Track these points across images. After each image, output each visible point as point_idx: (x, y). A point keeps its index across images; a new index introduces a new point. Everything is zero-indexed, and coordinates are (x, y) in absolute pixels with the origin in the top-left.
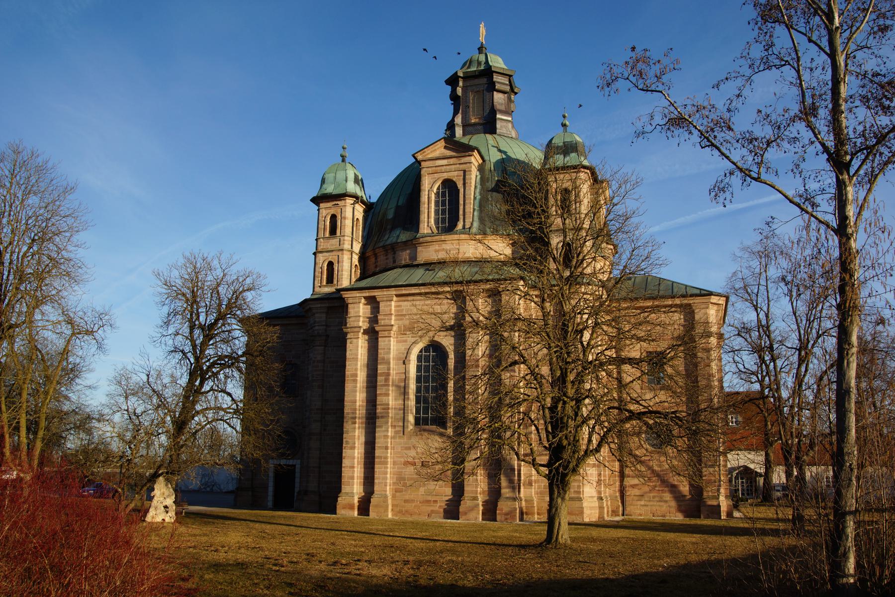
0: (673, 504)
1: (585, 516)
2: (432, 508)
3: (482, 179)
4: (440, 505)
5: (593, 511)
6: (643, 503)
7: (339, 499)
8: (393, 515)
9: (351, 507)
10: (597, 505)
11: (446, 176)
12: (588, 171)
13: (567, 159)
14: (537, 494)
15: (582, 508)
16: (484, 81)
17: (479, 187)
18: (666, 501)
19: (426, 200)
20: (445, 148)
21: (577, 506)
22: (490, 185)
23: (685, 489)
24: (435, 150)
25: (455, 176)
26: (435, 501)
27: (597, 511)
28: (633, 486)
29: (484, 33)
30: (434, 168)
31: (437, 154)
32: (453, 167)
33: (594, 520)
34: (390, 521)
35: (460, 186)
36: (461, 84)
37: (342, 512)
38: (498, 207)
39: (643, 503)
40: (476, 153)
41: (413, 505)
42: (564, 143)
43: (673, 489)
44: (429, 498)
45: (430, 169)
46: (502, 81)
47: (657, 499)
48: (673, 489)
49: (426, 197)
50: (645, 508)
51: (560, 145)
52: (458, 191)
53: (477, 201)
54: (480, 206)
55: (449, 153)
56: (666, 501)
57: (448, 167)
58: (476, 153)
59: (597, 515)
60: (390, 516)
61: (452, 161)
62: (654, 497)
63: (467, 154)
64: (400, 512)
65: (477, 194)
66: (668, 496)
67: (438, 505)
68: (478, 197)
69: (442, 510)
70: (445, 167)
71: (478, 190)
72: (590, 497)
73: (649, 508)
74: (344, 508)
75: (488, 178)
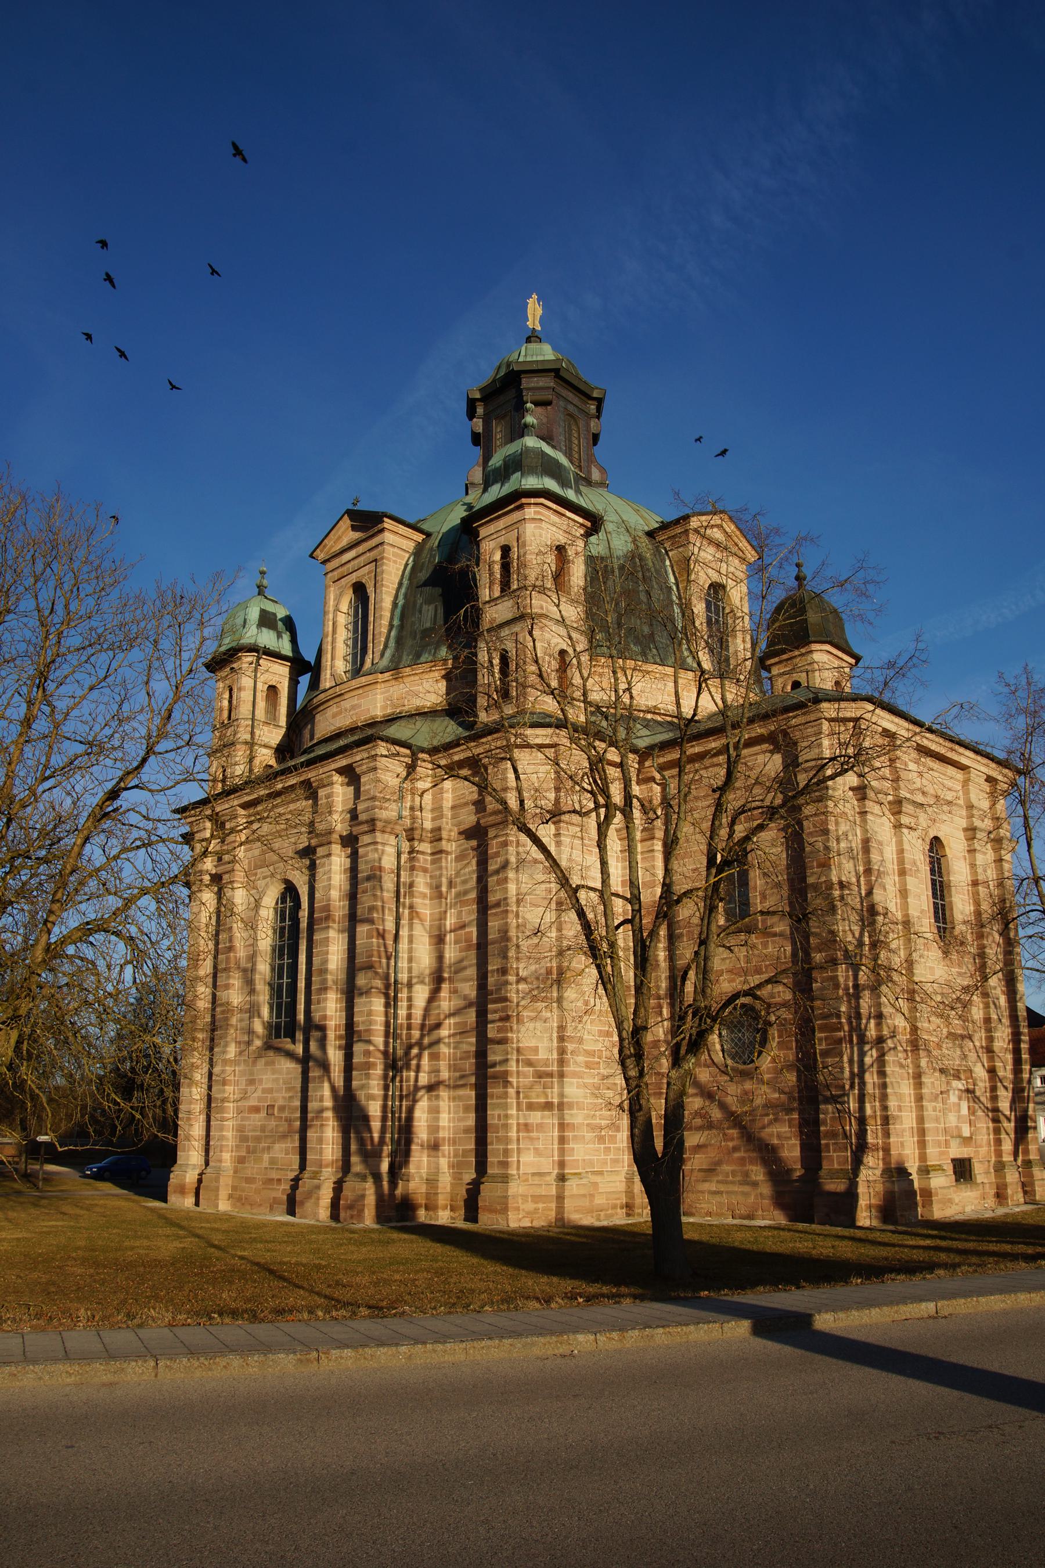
0: (766, 1189)
1: (511, 1215)
2: (274, 1194)
3: (413, 568)
4: (281, 1191)
5: (541, 1206)
6: (713, 1187)
7: (172, 1175)
8: (234, 1205)
9: (182, 1190)
10: (554, 1192)
11: (353, 578)
12: (542, 500)
13: (507, 485)
14: (453, 1167)
15: (506, 1197)
16: (511, 394)
17: (406, 582)
18: (755, 1184)
19: (330, 629)
20: (354, 528)
21: (499, 1194)
22: (424, 576)
23: (791, 1152)
24: (340, 537)
25: (364, 575)
26: (279, 1180)
27: (553, 1205)
28: (698, 1148)
29: (539, 311)
30: (340, 570)
31: (344, 542)
32: (362, 559)
33: (539, 1223)
34: (225, 1214)
35: (370, 590)
36: (480, 410)
37: (173, 1198)
38: (429, 614)
39: (713, 1187)
40: (388, 523)
41: (253, 1186)
42: (504, 460)
43: (768, 1154)
44: (274, 1175)
45: (335, 573)
46: (541, 384)
47: (739, 1178)
48: (768, 1154)
49: (331, 623)
50: (718, 1198)
51: (498, 465)
52: (368, 598)
53: (398, 611)
54: (402, 618)
55: (357, 535)
56: (755, 1184)
57: (356, 562)
58: (388, 523)
59: (553, 1214)
60: (224, 1206)
61: (361, 549)
62: (734, 1173)
63: (376, 529)
64: (240, 1199)
65: (401, 597)
66: (758, 1173)
67: (282, 1187)
68: (401, 602)
69: (285, 1197)
70: (352, 563)
71: (403, 590)
72: (534, 1174)
73: (725, 1199)
74: (175, 1192)
75: (423, 563)
